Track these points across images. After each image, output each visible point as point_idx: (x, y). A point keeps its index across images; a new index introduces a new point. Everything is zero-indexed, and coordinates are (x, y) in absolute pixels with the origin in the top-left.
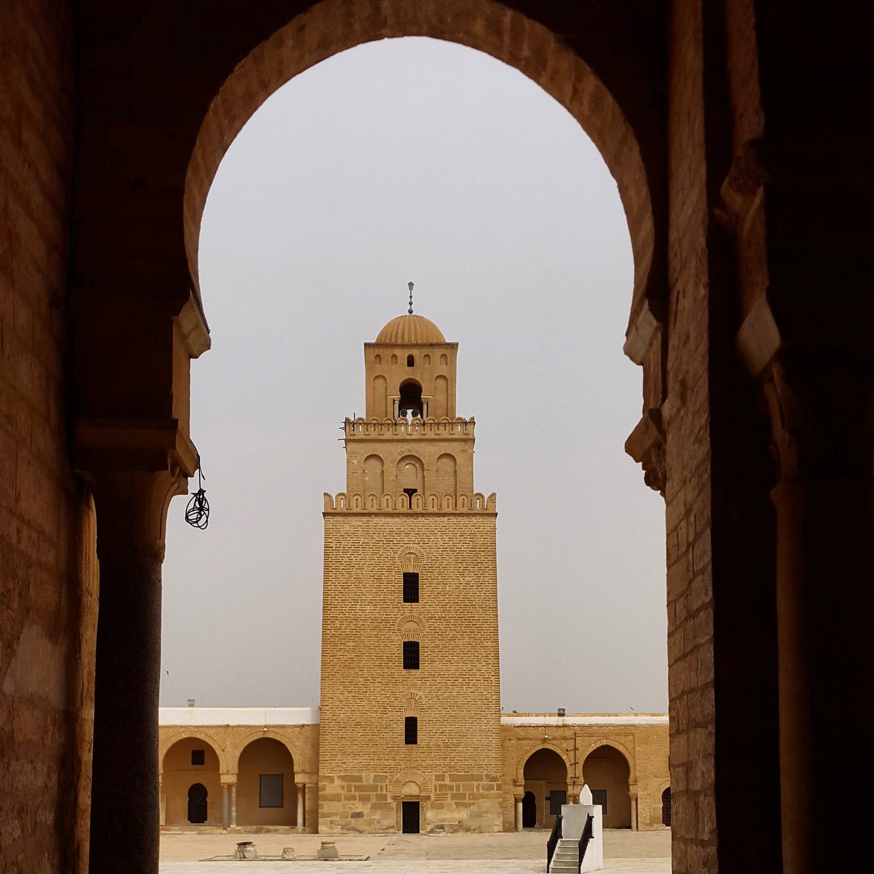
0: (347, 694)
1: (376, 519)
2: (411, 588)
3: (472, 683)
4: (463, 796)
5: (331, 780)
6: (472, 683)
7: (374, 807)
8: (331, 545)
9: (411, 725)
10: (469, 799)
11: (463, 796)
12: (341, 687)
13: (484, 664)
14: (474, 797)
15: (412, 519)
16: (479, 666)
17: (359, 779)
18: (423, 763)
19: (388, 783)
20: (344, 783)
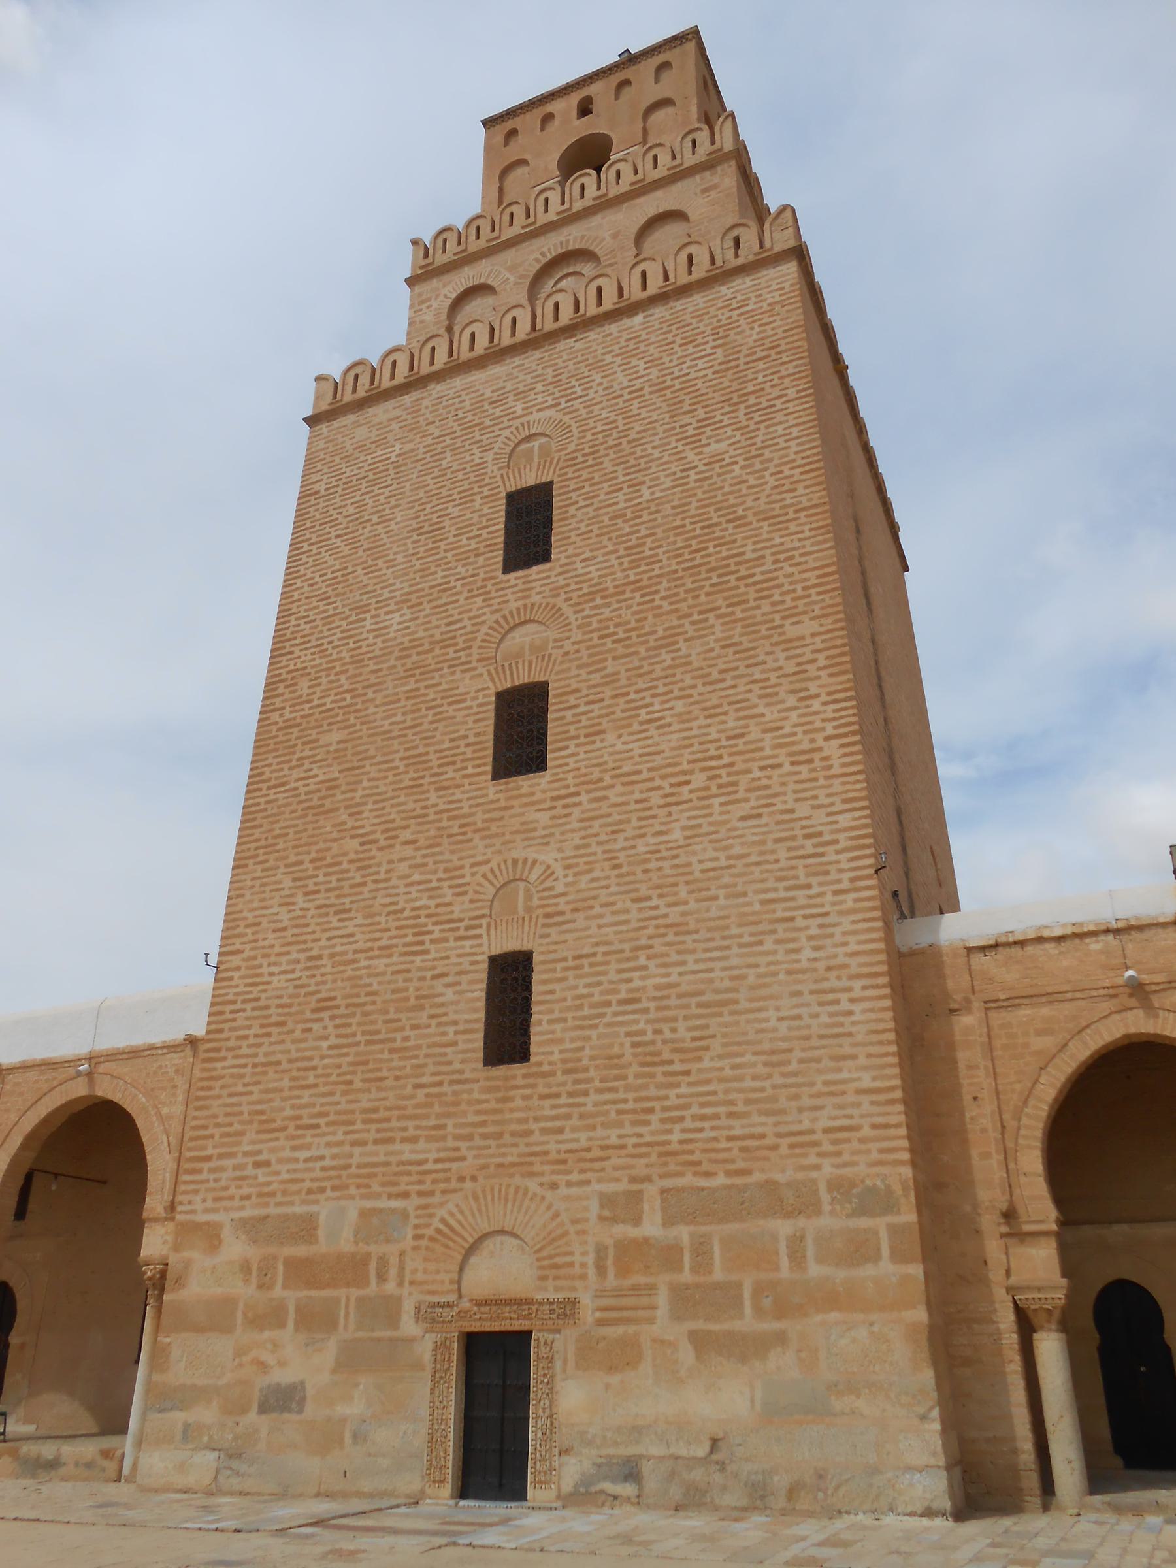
0: (300, 900)
1: (439, 387)
2: (529, 529)
3: (744, 781)
4: (726, 1298)
5: (211, 1237)
6: (744, 781)
7: (351, 1361)
8: (316, 487)
9: (511, 979)
10: (759, 1311)
11: (726, 1298)
12: (287, 883)
13: (791, 701)
14: (783, 1303)
15: (537, 354)
16: (771, 714)
17: (306, 1228)
18: (553, 1146)
19: (409, 1242)
20: (253, 1253)
